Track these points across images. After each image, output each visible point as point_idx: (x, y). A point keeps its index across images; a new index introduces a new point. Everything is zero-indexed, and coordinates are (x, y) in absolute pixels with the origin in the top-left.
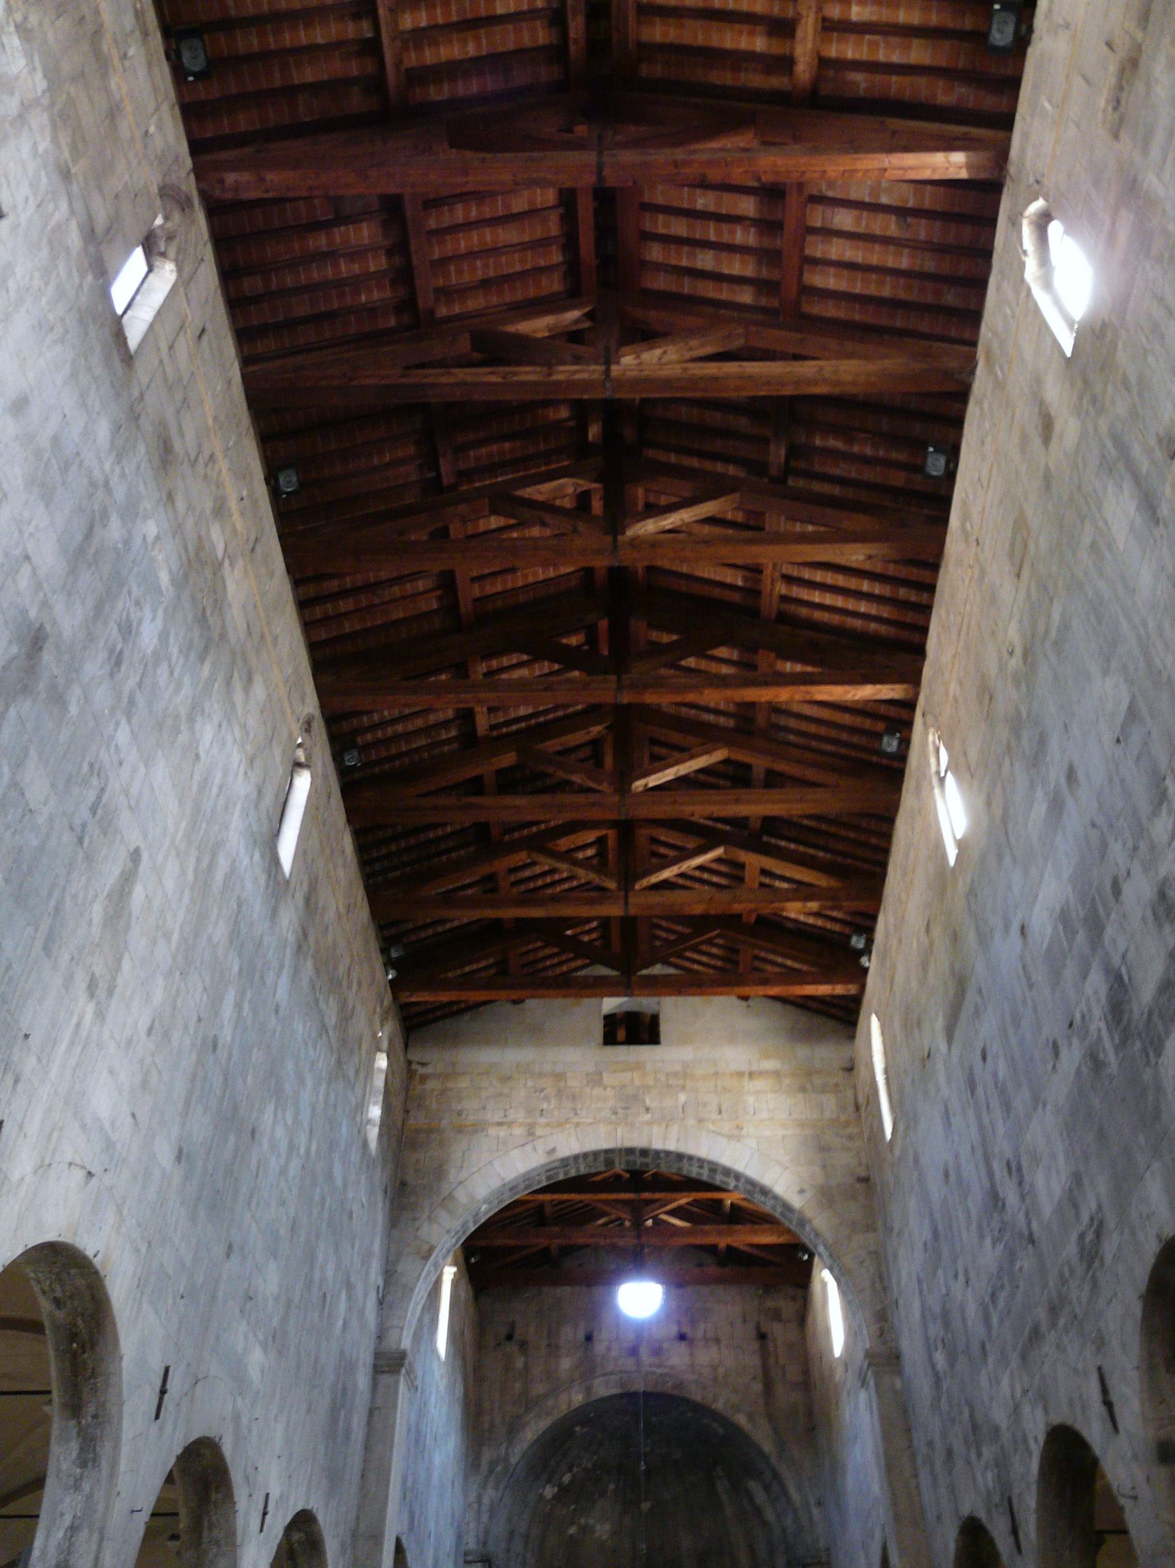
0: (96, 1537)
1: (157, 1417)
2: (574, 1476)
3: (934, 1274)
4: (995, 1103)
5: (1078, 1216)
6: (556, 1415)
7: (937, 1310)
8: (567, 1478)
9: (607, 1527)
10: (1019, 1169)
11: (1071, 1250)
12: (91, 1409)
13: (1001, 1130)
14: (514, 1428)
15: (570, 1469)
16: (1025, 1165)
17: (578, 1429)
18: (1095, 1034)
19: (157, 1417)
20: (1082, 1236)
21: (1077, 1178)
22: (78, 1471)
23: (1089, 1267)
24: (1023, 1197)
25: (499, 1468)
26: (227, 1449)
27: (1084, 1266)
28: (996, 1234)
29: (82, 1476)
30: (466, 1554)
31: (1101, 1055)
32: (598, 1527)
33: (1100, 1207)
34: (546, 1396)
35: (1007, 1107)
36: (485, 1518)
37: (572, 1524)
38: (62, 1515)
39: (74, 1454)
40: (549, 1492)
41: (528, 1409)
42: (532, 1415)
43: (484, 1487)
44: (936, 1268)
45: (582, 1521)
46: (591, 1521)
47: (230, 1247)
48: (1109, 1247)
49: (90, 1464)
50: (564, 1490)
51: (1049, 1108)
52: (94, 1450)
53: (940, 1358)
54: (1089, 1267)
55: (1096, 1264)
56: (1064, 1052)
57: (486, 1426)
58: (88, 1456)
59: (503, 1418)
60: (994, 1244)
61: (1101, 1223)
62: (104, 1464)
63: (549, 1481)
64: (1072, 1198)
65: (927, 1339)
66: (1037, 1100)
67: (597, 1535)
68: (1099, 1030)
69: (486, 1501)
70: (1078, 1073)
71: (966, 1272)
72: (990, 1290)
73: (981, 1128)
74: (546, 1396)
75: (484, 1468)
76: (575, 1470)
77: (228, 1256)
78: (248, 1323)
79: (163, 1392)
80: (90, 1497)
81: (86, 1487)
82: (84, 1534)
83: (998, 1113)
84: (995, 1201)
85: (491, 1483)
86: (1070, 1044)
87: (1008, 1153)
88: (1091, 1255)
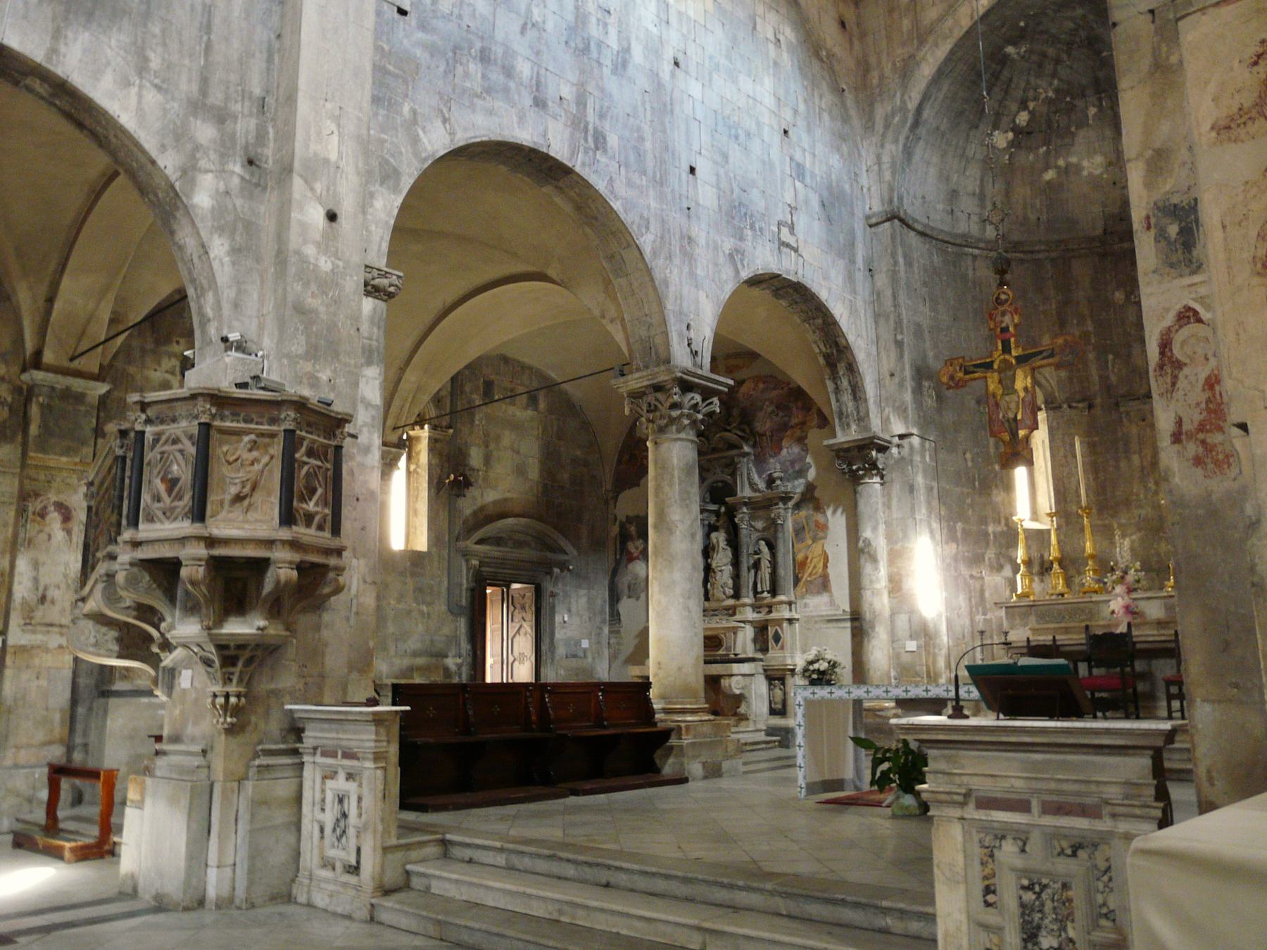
2: (1032, 113)
6: (958, 33)
8: (1023, 118)
9: (1099, 159)
14: (906, 70)
15: (1023, 105)
17: (1010, 50)
25: (897, 119)
30: (868, 218)
32: (1085, 163)
34: (941, 19)
36: (887, 176)
37: (1047, 167)
40: (1001, 139)
41: (922, 42)
42: (927, 46)
43: (882, 146)
45: (1061, 162)
46: (1074, 160)
50: (1022, 136)
57: (875, 81)
59: (894, 64)
63: (996, 127)
67: (1085, 173)
69: (886, 159)
74: (941, 19)
75: (879, 126)
76: (1031, 105)
85: (890, 135)
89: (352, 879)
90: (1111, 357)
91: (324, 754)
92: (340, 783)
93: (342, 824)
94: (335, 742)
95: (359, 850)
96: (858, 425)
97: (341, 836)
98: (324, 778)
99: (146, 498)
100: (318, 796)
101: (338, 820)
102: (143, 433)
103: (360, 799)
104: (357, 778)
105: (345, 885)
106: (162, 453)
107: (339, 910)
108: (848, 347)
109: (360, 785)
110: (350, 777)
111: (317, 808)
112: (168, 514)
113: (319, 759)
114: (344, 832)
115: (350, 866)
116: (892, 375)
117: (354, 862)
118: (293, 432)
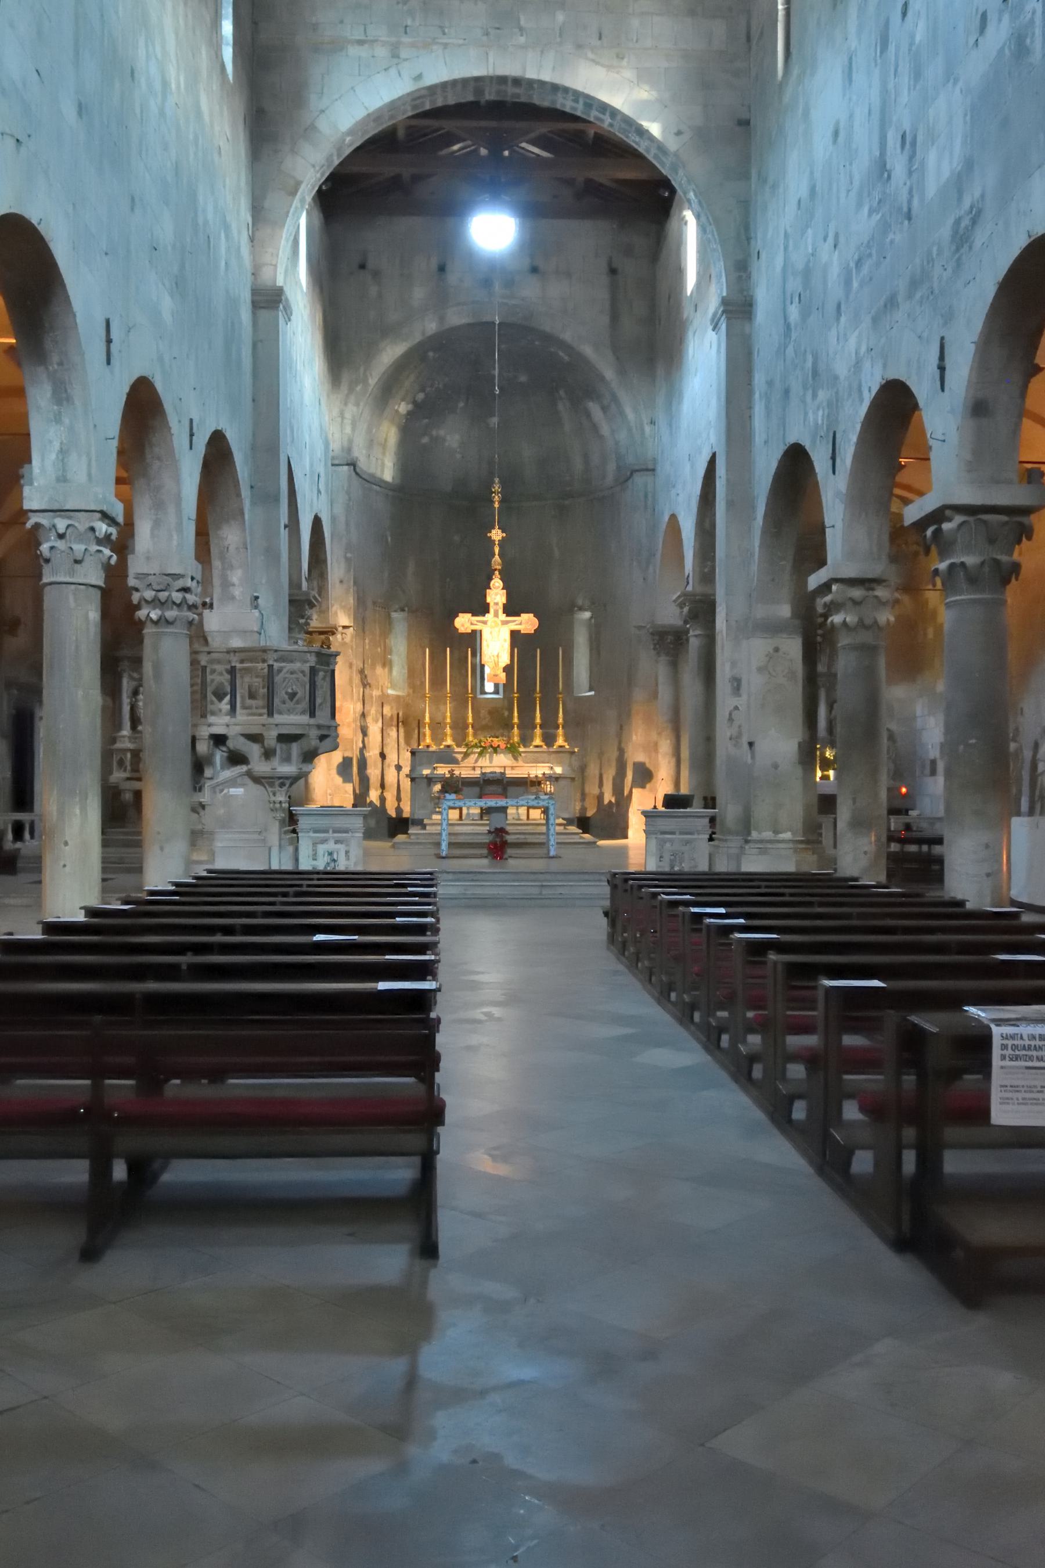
0: (84, 458)
1: (109, 362)
3: (803, 232)
4: (905, 68)
5: (960, 199)
7: (800, 266)
10: (914, 143)
11: (945, 232)
12: (55, 358)
13: (904, 98)
16: (920, 138)
18: (1029, 16)
19: (109, 362)
20: (958, 222)
21: (969, 164)
22: (55, 407)
23: (957, 250)
24: (910, 173)
26: (159, 386)
27: (954, 248)
28: (875, 204)
29: (60, 413)
31: (1028, 41)
33: (983, 196)
35: (917, 74)
38: (50, 442)
39: (49, 394)
44: (807, 227)
47: (133, 199)
48: (980, 238)
49: (65, 403)
51: (960, 84)
52: (66, 391)
53: (794, 312)
54: (957, 250)
55: (966, 247)
56: (991, 29)
58: (61, 395)
60: (871, 212)
61: (979, 212)
62: (78, 403)
64: (959, 183)
65: (784, 292)
66: (950, 76)
68: (1034, 12)
70: (1001, 51)
71: (837, 236)
72: (856, 257)
73: (884, 91)
77: (132, 209)
78: (156, 273)
79: (109, 341)
80: (71, 429)
81: (67, 421)
82: (73, 457)
83: (905, 80)
84: (882, 169)
86: (1000, 20)
87: (907, 126)
88: (962, 239)
90: (448, 580)
91: (316, 831)
92: (331, 846)
96: (319, 616)
98: (315, 844)
99: (277, 701)
100: (311, 853)
102: (273, 665)
103: (347, 852)
106: (285, 678)
108: (325, 561)
110: (336, 842)
111: (311, 858)
112: (289, 712)
113: (312, 834)
116: (341, 582)
118: (314, 667)
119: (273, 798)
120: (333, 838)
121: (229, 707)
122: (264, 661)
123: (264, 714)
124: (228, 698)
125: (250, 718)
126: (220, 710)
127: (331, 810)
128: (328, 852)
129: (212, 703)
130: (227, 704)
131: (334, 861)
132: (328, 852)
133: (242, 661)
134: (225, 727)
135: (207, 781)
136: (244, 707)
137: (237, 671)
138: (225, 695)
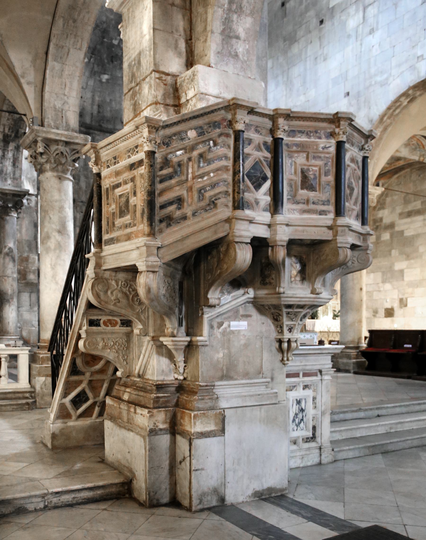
89: (313, 444)
92: (299, 393)
93: (300, 416)
94: (301, 368)
95: (314, 428)
97: (300, 423)
101: (296, 414)
103: (314, 399)
104: (312, 387)
105: (309, 449)
107: (309, 464)
109: (314, 391)
110: (306, 387)
114: (302, 420)
115: (307, 438)
117: (310, 434)
119: (287, 335)
120: (303, 382)
121: (268, 199)
122: (332, 135)
123: (329, 212)
124: (268, 184)
125: (306, 216)
126: (257, 203)
127: (309, 349)
128: (297, 400)
129: (248, 190)
130: (265, 194)
131: (302, 410)
132: (297, 400)
133: (292, 133)
134: (266, 227)
135: (206, 309)
136: (294, 200)
137: (284, 147)
138: (265, 179)
